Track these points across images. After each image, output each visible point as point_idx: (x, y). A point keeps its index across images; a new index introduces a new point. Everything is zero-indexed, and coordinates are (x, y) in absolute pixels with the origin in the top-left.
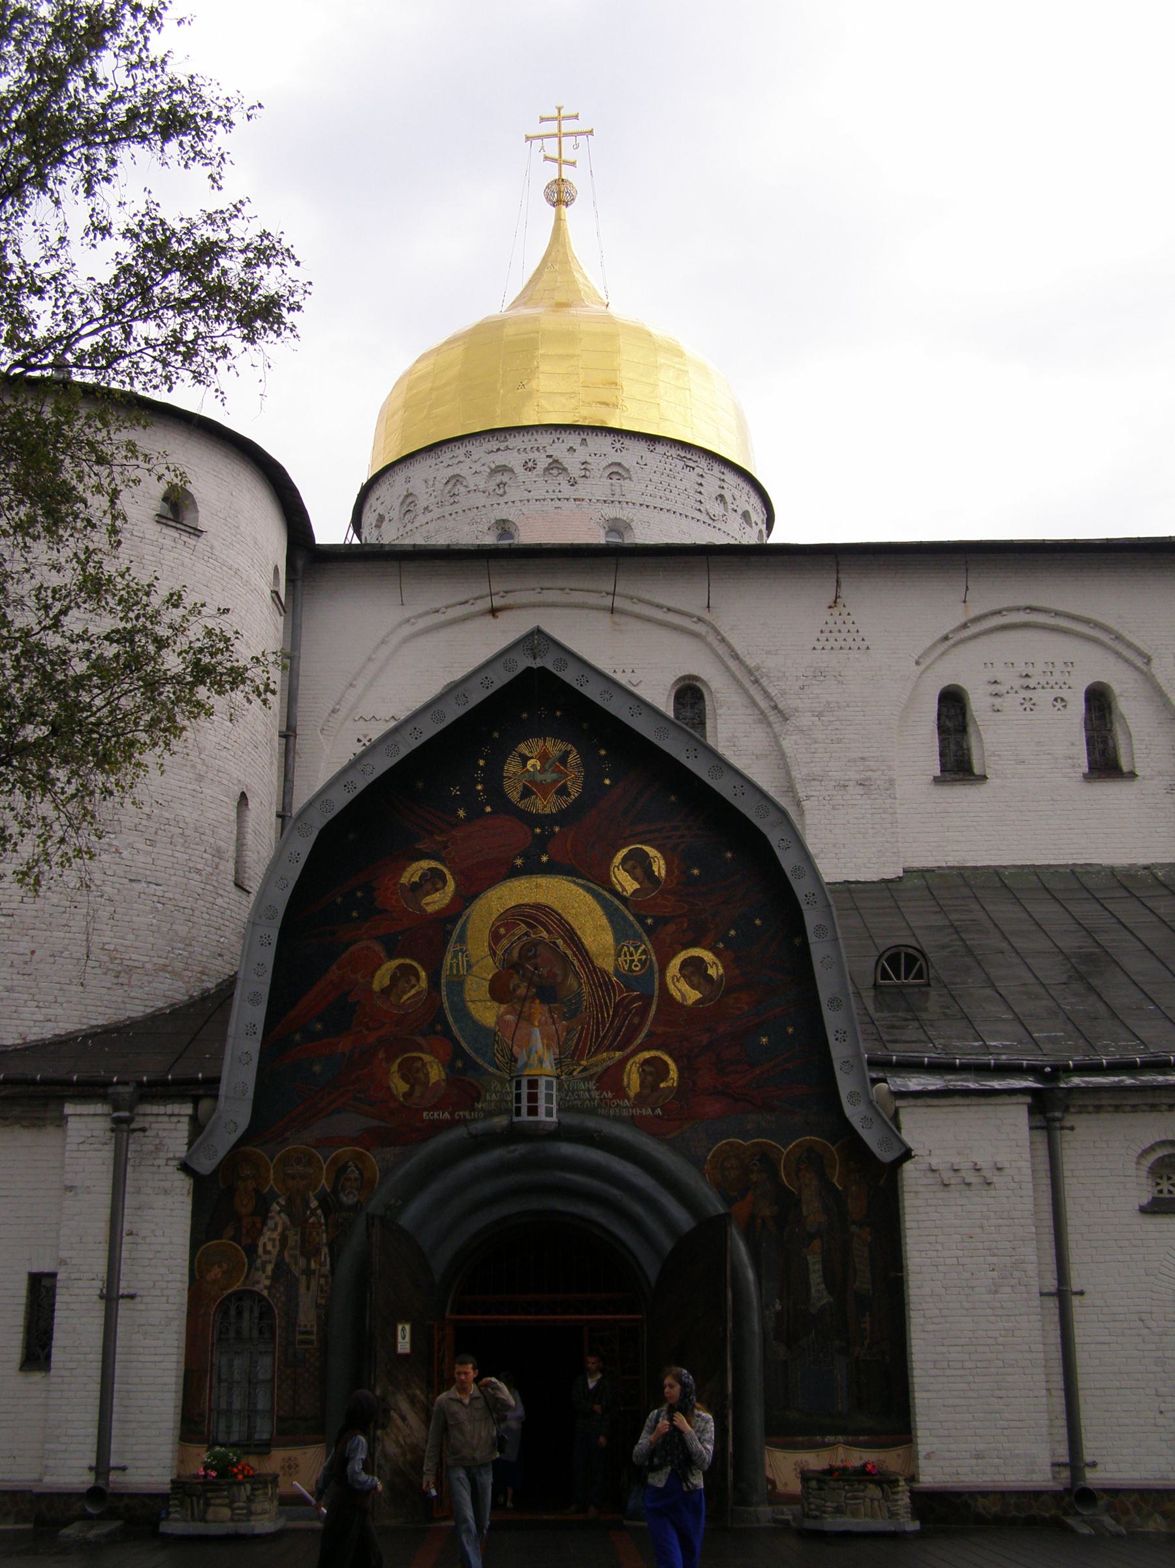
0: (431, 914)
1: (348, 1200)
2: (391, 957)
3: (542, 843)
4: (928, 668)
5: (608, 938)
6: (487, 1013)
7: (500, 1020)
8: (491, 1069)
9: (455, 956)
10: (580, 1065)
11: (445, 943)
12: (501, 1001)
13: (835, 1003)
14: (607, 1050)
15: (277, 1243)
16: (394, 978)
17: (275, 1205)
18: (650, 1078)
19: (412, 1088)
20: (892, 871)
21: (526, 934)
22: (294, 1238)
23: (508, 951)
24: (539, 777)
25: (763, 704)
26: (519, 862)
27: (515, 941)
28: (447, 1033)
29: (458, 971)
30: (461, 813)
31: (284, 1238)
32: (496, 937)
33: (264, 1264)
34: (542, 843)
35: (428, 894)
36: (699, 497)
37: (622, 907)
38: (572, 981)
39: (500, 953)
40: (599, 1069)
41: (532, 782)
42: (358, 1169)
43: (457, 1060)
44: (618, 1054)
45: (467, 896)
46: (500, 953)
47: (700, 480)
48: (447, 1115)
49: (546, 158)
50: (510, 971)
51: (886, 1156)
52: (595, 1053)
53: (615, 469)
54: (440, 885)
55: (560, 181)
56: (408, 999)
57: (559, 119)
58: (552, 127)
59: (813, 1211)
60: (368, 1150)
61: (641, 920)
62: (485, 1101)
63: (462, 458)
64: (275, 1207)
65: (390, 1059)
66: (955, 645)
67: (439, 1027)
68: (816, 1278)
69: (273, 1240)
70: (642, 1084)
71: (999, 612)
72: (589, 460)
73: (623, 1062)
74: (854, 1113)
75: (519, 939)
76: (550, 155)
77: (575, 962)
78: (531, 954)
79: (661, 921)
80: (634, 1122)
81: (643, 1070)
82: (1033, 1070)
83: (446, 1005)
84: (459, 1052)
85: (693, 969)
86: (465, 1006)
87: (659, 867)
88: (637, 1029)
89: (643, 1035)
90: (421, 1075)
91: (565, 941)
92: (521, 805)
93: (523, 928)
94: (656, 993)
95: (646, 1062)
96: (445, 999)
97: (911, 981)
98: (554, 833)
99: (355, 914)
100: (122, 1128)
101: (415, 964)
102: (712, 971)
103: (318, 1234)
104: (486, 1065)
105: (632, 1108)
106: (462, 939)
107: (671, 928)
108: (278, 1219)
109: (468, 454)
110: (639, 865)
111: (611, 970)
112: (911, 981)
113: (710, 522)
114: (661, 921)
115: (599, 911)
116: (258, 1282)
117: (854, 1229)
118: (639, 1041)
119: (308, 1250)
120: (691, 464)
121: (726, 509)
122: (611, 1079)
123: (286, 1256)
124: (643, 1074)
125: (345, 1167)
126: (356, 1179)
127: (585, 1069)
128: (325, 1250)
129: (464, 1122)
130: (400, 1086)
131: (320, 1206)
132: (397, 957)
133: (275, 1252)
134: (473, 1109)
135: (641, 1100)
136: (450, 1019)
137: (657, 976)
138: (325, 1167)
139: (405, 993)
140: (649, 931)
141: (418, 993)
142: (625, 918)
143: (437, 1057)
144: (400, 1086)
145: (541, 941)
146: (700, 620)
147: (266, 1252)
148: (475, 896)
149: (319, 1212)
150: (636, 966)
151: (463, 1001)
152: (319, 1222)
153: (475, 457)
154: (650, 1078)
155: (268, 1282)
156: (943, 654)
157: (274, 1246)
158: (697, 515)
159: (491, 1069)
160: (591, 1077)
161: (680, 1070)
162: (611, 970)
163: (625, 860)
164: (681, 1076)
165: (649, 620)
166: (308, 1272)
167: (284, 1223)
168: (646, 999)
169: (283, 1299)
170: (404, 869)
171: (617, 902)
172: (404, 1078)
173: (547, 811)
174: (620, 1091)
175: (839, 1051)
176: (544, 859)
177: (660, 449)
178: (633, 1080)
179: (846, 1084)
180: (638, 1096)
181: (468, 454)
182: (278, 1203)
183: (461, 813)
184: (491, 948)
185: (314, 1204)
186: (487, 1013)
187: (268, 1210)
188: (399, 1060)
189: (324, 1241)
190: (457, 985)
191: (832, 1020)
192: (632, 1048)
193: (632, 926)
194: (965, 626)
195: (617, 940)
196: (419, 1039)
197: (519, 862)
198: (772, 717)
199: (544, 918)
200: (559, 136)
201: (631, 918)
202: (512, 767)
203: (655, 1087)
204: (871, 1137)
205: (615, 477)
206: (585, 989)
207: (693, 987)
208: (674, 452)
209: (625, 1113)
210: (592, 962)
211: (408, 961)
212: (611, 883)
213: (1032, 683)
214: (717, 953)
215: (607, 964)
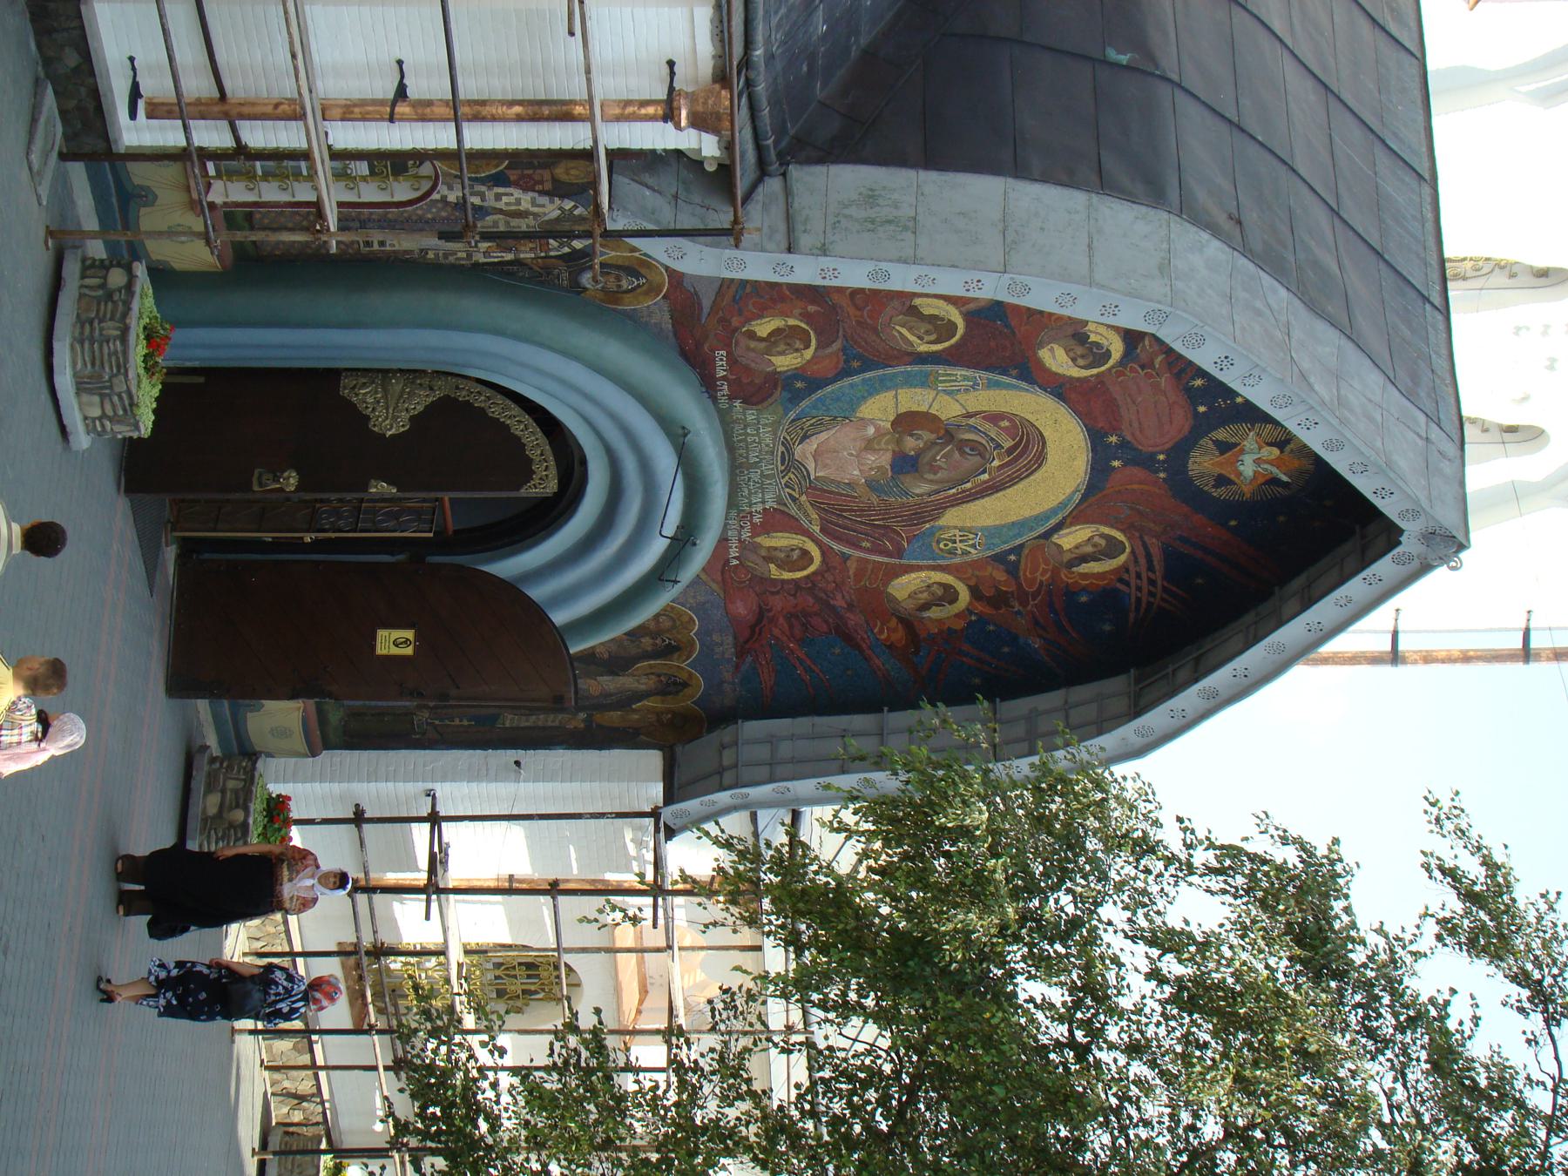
0: (1035, 354)
8: (792, 415)
9: (965, 378)
10: (801, 494)
11: (986, 369)
14: (821, 518)
15: (513, 208)
17: (573, 204)
19: (761, 340)
26: (1113, 439)
27: (987, 436)
29: (941, 382)
32: (994, 418)
33: (482, 196)
35: (1068, 351)
38: (921, 488)
39: (972, 421)
40: (794, 511)
42: (633, 289)
44: (817, 529)
45: (1060, 389)
46: (972, 421)
50: (942, 432)
54: (1081, 362)
56: (900, 333)
60: (664, 297)
62: (744, 409)
64: (568, 205)
65: (806, 317)
69: (518, 202)
70: (776, 549)
75: (992, 439)
77: (954, 491)
78: (967, 450)
80: (723, 541)
81: (793, 550)
83: (889, 371)
86: (888, 389)
89: (845, 550)
90: (782, 347)
91: (985, 482)
93: (1008, 443)
94: (903, 561)
96: (902, 369)
98: (1157, 471)
101: (953, 341)
103: (531, 249)
105: (740, 540)
106: (998, 385)
115: (1027, 513)
116: (450, 188)
118: (836, 546)
123: (496, 217)
125: (637, 275)
126: (620, 286)
127: (794, 499)
128: (509, 257)
131: (575, 251)
133: (501, 205)
134: (731, 398)
136: (868, 375)
137: (931, 562)
139: (910, 329)
143: (809, 362)
147: (498, 197)
149: (566, 250)
150: (946, 545)
151: (896, 387)
152: (550, 250)
154: (783, 555)
155: (452, 198)
157: (506, 204)
159: (792, 415)
162: (941, 522)
167: (545, 214)
168: (899, 553)
169: (429, 216)
176: (1116, 463)
180: (760, 546)
182: (575, 207)
184: (980, 412)
187: (562, 197)
188: (803, 325)
189: (522, 256)
192: (826, 540)
195: (982, 529)
196: (836, 346)
199: (1023, 462)
201: (1018, 542)
203: (769, 559)
210: (953, 506)
212: (1072, 524)
215: (952, 518)
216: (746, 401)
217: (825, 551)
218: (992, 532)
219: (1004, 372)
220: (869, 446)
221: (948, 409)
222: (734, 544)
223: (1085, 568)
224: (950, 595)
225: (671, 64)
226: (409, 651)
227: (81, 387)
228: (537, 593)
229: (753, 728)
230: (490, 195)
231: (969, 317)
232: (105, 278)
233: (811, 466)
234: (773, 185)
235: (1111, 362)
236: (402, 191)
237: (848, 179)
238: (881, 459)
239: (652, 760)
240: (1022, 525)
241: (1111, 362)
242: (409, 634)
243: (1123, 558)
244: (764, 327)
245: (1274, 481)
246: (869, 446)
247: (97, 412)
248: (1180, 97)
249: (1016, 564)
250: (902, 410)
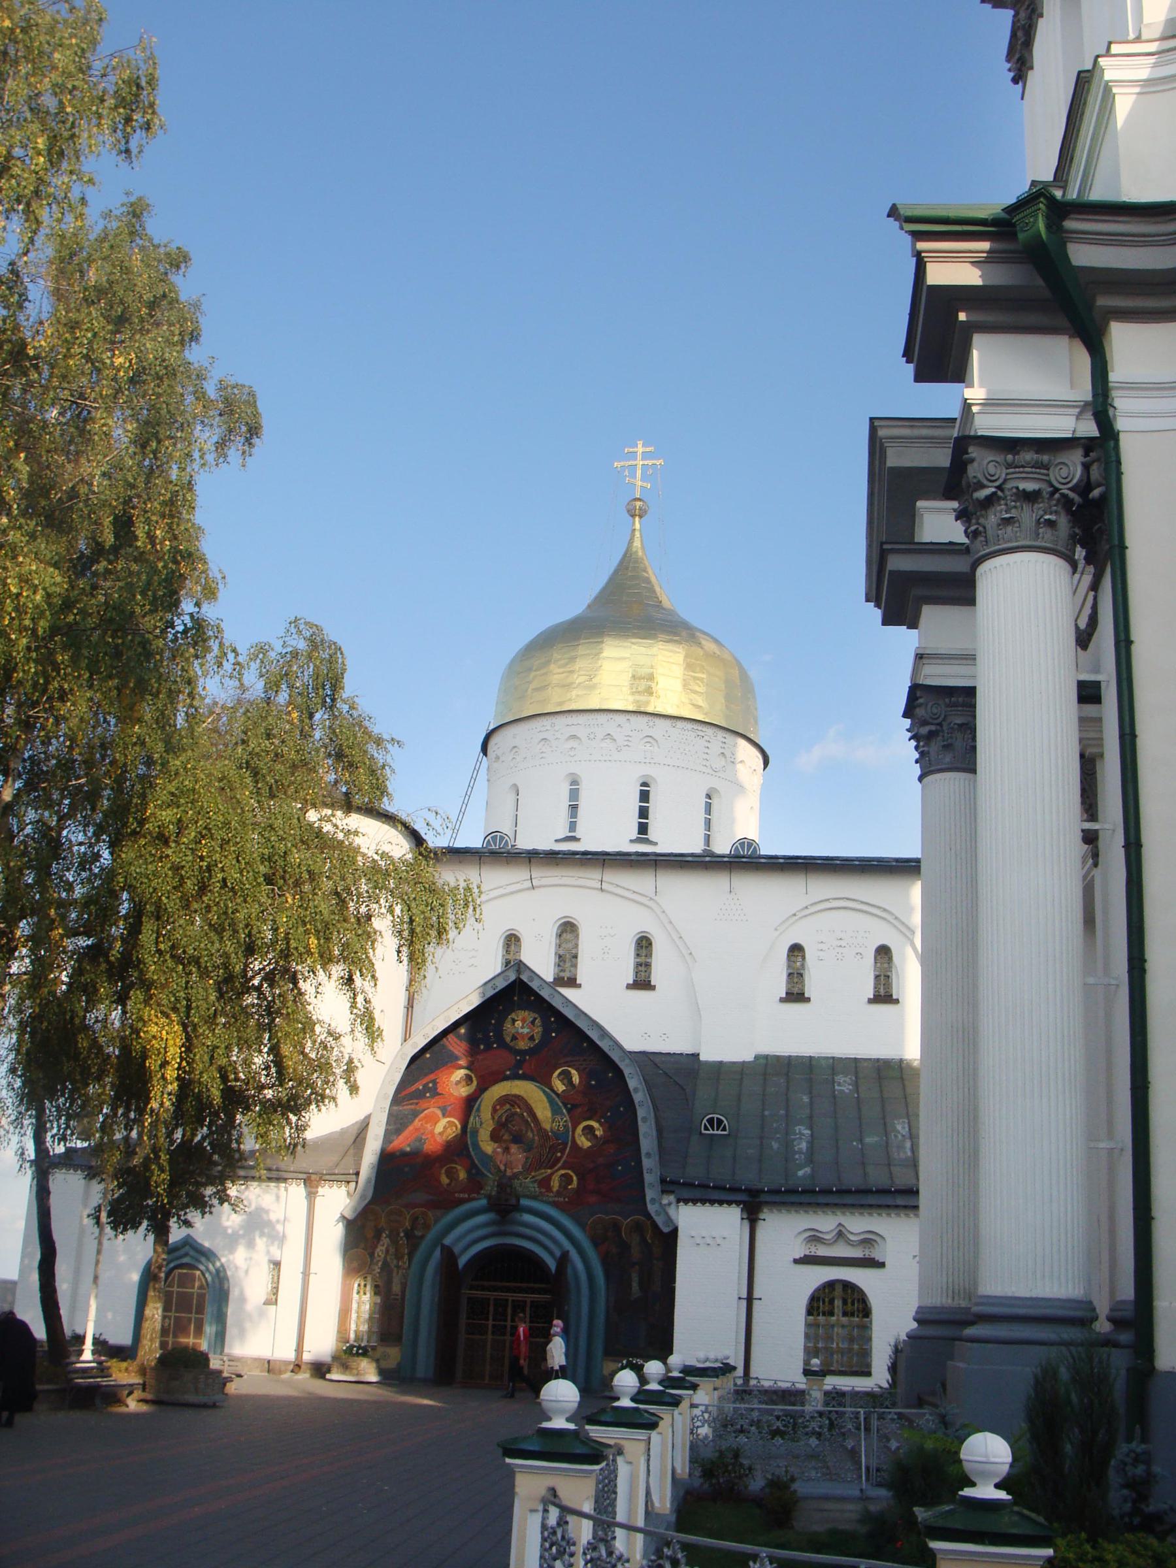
1: (418, 1233)
2: (444, 1116)
3: (519, 1065)
4: (781, 934)
5: (549, 1114)
6: (488, 1147)
7: (494, 1151)
12: (496, 1142)
13: (648, 1155)
14: (545, 1168)
18: (563, 1184)
19: (451, 1181)
20: (749, 1057)
21: (509, 1109)
22: (392, 1250)
23: (500, 1117)
24: (521, 1031)
25: (685, 952)
28: (469, 1156)
30: (482, 1047)
31: (387, 1251)
32: (494, 1110)
34: (519, 1065)
36: (705, 756)
37: (557, 1099)
38: (530, 1134)
39: (496, 1118)
40: (540, 1178)
41: (517, 1033)
43: (472, 1169)
44: (549, 1171)
47: (708, 745)
48: (466, 1196)
51: (666, 1230)
52: (540, 1169)
53: (649, 739)
59: (636, 1252)
61: (565, 1105)
63: (549, 728)
65: (442, 1167)
66: (801, 918)
68: (635, 1285)
70: (560, 1186)
71: (827, 900)
72: (630, 733)
73: (552, 1174)
74: (652, 1208)
79: (574, 1106)
80: (555, 1205)
82: (749, 1191)
84: (474, 1165)
85: (589, 1130)
87: (576, 1079)
88: (558, 1159)
92: (512, 1044)
93: (508, 1106)
95: (562, 1175)
97: (720, 1132)
98: (525, 1060)
99: (428, 1095)
100: (311, 1196)
102: (598, 1133)
104: (485, 1172)
106: (478, 1110)
107: (580, 1110)
108: (385, 1241)
109: (553, 725)
110: (566, 1077)
111: (549, 1129)
112: (720, 1132)
113: (710, 771)
114: (574, 1106)
115: (545, 1099)
117: (655, 1262)
118: (560, 1165)
119: (399, 1257)
120: (703, 734)
121: (726, 761)
122: (545, 1183)
124: (561, 1181)
125: (417, 1218)
127: (533, 1177)
128: (406, 1257)
129: (474, 1199)
130: (445, 1180)
132: (448, 1117)
134: (478, 1193)
135: (558, 1193)
138: (408, 1217)
140: (569, 1111)
142: (558, 1105)
144: (445, 1180)
145: (516, 1113)
146: (651, 899)
147: (379, 1256)
148: (486, 1089)
151: (477, 1141)
153: (557, 728)
156: (794, 923)
158: (704, 769)
160: (535, 1181)
161: (579, 1179)
162: (549, 1129)
163: (560, 1074)
164: (579, 1184)
165: (622, 897)
166: (398, 1267)
168: (565, 1144)
170: (453, 1073)
171: (554, 1095)
172: (447, 1176)
173: (523, 1048)
174: (549, 1189)
175: (649, 1178)
177: (680, 724)
178: (555, 1184)
179: (650, 1194)
181: (553, 725)
183: (482, 1047)
185: (402, 1235)
186: (488, 1147)
190: (475, 1132)
191: (646, 1163)
193: (560, 1108)
194: (806, 907)
195: (553, 1115)
197: (508, 1073)
198: (688, 958)
201: (561, 1104)
202: (508, 1025)
203: (566, 1188)
204: (659, 1220)
205: (648, 745)
206: (536, 1138)
207: (587, 1139)
208: (689, 726)
209: (551, 1199)
213: (843, 943)
214: (601, 1124)
215: (547, 1126)
216: (481, 1188)
217: (562, 1168)
222: (556, 1199)
238: (514, 1148)
240: (551, 1102)
249: (573, 1105)
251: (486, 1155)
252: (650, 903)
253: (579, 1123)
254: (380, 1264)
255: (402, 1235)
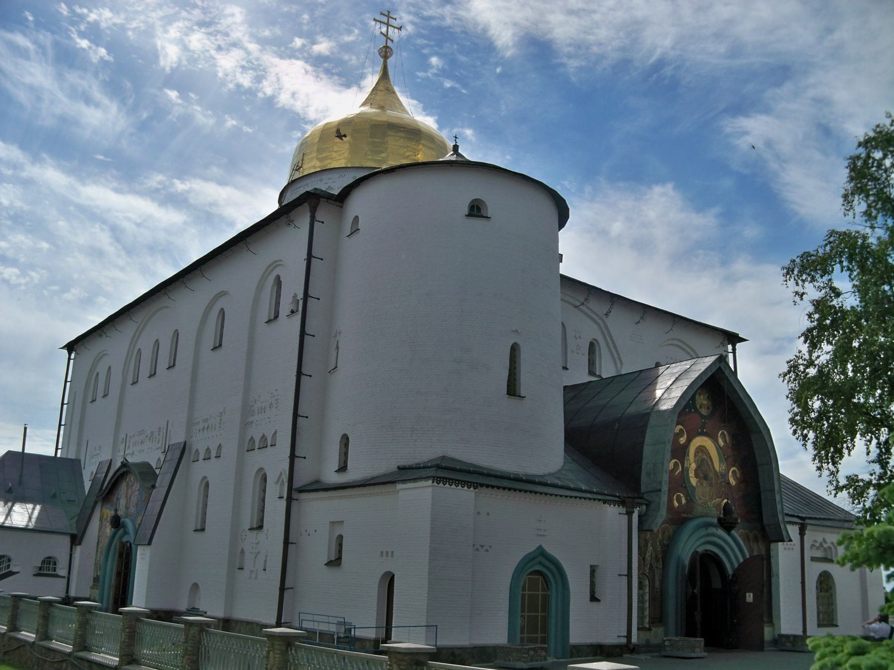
16: (674, 465)
31: (651, 556)
32: (695, 456)
33: (647, 564)
35: (681, 437)
45: (689, 441)
49: (381, 33)
55: (386, 47)
57: (388, 17)
58: (385, 19)
64: (649, 544)
67: (684, 485)
69: (649, 556)
76: (383, 32)
125: (664, 531)
128: (661, 560)
133: (649, 560)
141: (679, 472)
147: (648, 560)
155: (648, 571)
162: (718, 471)
176: (705, 430)
185: (658, 544)
187: (647, 546)
190: (688, 470)
200: (388, 25)
201: (722, 455)
206: (713, 476)
211: (678, 462)
212: (718, 442)
218: (720, 461)
219: (685, 452)
220: (702, 484)
221: (693, 466)
223: (728, 441)
224: (734, 472)
225: (620, 514)
226: (752, 594)
227: (693, 652)
228: (736, 565)
229: (765, 522)
230: (647, 562)
231: (674, 458)
232: (667, 646)
233: (706, 499)
234: (646, 496)
235: (683, 428)
236: (647, 582)
237: (644, 477)
239: (773, 545)
240: (718, 453)
241: (683, 428)
242: (747, 594)
243: (725, 432)
244: (676, 504)
245: (708, 397)
246: (702, 484)
247: (699, 650)
248: (626, 413)
250: (694, 476)
251: (693, 486)
252: (600, 322)
253: (730, 470)
254: (648, 565)
255: (658, 544)
